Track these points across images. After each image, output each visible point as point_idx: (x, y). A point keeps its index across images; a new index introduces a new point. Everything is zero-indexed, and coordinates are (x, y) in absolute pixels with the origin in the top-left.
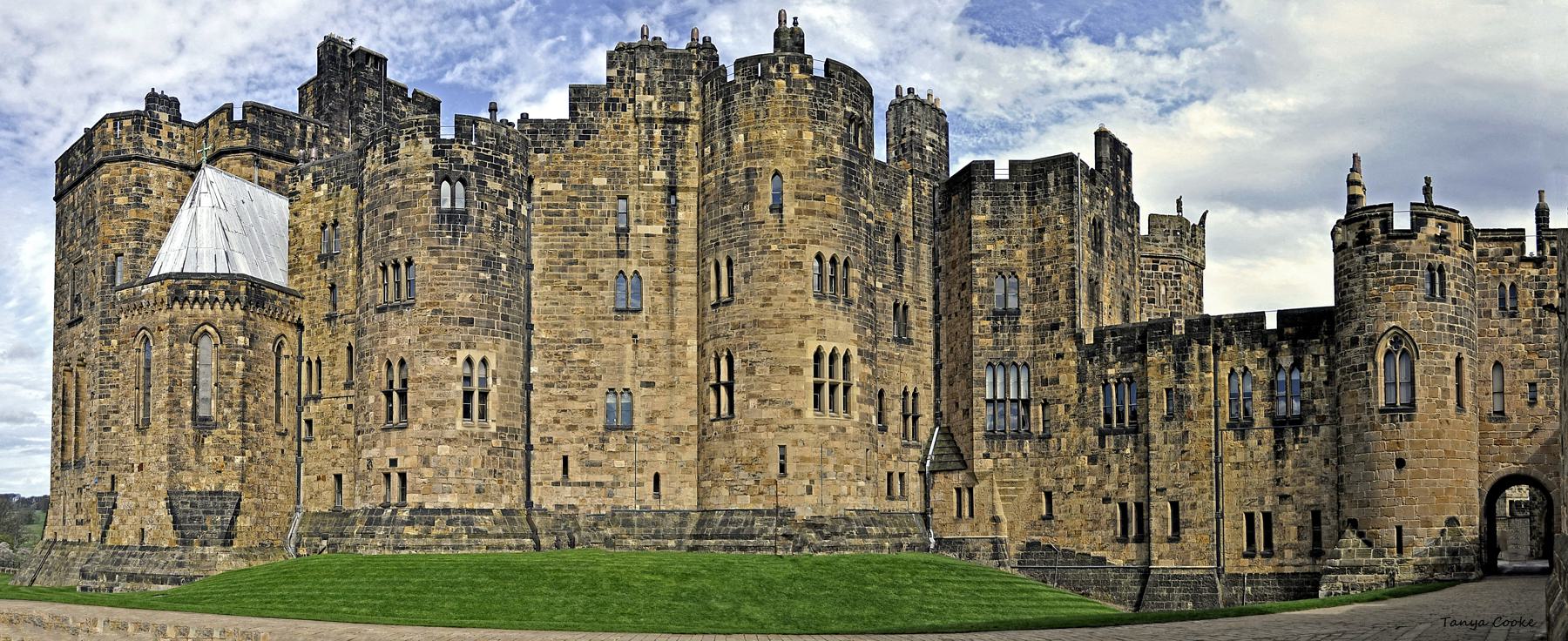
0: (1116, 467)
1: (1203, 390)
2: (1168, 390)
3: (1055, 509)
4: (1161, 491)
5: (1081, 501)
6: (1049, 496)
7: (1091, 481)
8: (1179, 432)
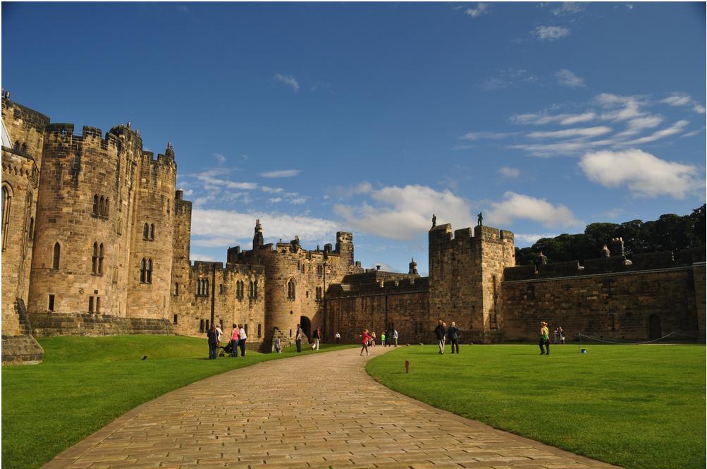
2: (221, 285)
3: (178, 321)
4: (217, 316)
6: (176, 316)
7: (192, 312)
8: (224, 298)
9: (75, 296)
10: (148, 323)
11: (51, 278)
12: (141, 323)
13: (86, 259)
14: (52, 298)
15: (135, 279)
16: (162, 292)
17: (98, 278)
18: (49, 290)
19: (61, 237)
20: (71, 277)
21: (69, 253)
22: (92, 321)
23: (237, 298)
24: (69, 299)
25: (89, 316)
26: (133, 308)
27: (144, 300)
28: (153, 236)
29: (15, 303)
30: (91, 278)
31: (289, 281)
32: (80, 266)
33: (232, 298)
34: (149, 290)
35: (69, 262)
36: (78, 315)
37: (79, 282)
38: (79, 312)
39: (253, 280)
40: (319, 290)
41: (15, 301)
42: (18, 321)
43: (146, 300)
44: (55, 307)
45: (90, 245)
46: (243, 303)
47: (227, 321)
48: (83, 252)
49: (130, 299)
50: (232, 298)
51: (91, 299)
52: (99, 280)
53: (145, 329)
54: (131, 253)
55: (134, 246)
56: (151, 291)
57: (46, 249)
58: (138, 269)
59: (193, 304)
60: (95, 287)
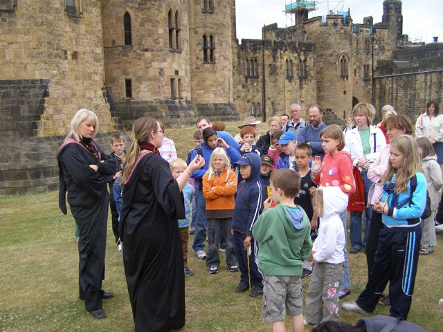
0: (251, 90)
1: (281, 65)
5: (240, 102)
7: (243, 94)
8: (274, 79)
9: (155, 79)
10: (215, 109)
11: (125, 58)
12: (208, 108)
13: (162, 30)
14: (128, 83)
15: (197, 58)
16: (226, 73)
17: (177, 55)
18: (125, 72)
19: (130, 4)
20: (148, 54)
21: (142, 24)
22: (176, 108)
23: (287, 78)
24: (148, 83)
25: (173, 102)
26: (197, 92)
27: (208, 82)
28: (212, 8)
29: (103, 89)
30: (170, 55)
31: (341, 58)
32: (156, 41)
33: (282, 79)
34: (214, 71)
35: (143, 36)
36: (161, 102)
37: (157, 60)
38: (161, 98)
39: (302, 58)
40: (366, 67)
41: (102, 85)
42: (109, 113)
43: (211, 82)
44: (134, 94)
45: (164, 14)
46: (293, 83)
47: (279, 104)
48: (158, 22)
49: (195, 82)
50: (282, 79)
51: (172, 80)
52: (179, 57)
53: (213, 115)
54: (190, 29)
55: (192, 20)
56: (216, 72)
57: (115, 21)
58: (200, 47)
59: (243, 87)
60: (175, 66)
